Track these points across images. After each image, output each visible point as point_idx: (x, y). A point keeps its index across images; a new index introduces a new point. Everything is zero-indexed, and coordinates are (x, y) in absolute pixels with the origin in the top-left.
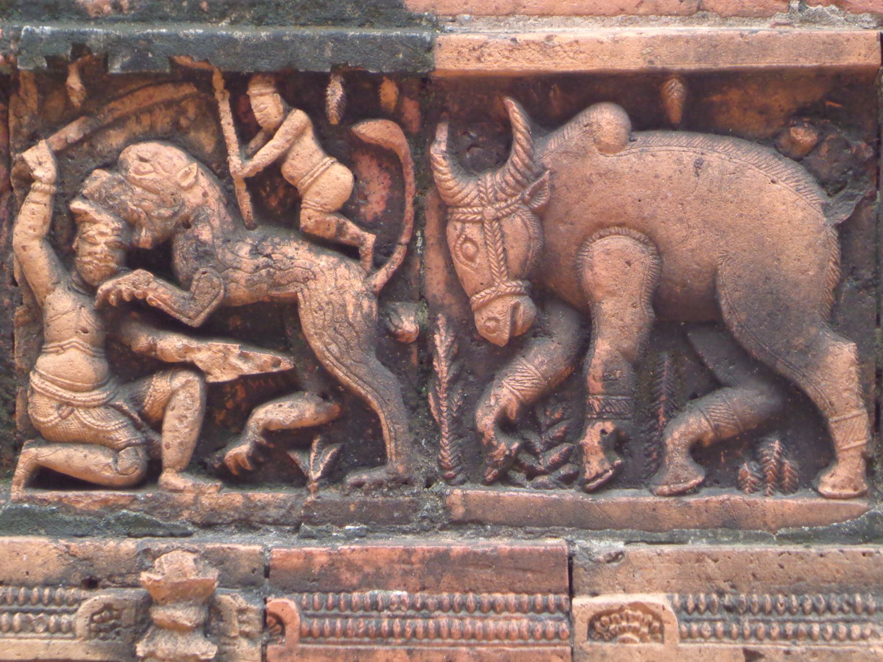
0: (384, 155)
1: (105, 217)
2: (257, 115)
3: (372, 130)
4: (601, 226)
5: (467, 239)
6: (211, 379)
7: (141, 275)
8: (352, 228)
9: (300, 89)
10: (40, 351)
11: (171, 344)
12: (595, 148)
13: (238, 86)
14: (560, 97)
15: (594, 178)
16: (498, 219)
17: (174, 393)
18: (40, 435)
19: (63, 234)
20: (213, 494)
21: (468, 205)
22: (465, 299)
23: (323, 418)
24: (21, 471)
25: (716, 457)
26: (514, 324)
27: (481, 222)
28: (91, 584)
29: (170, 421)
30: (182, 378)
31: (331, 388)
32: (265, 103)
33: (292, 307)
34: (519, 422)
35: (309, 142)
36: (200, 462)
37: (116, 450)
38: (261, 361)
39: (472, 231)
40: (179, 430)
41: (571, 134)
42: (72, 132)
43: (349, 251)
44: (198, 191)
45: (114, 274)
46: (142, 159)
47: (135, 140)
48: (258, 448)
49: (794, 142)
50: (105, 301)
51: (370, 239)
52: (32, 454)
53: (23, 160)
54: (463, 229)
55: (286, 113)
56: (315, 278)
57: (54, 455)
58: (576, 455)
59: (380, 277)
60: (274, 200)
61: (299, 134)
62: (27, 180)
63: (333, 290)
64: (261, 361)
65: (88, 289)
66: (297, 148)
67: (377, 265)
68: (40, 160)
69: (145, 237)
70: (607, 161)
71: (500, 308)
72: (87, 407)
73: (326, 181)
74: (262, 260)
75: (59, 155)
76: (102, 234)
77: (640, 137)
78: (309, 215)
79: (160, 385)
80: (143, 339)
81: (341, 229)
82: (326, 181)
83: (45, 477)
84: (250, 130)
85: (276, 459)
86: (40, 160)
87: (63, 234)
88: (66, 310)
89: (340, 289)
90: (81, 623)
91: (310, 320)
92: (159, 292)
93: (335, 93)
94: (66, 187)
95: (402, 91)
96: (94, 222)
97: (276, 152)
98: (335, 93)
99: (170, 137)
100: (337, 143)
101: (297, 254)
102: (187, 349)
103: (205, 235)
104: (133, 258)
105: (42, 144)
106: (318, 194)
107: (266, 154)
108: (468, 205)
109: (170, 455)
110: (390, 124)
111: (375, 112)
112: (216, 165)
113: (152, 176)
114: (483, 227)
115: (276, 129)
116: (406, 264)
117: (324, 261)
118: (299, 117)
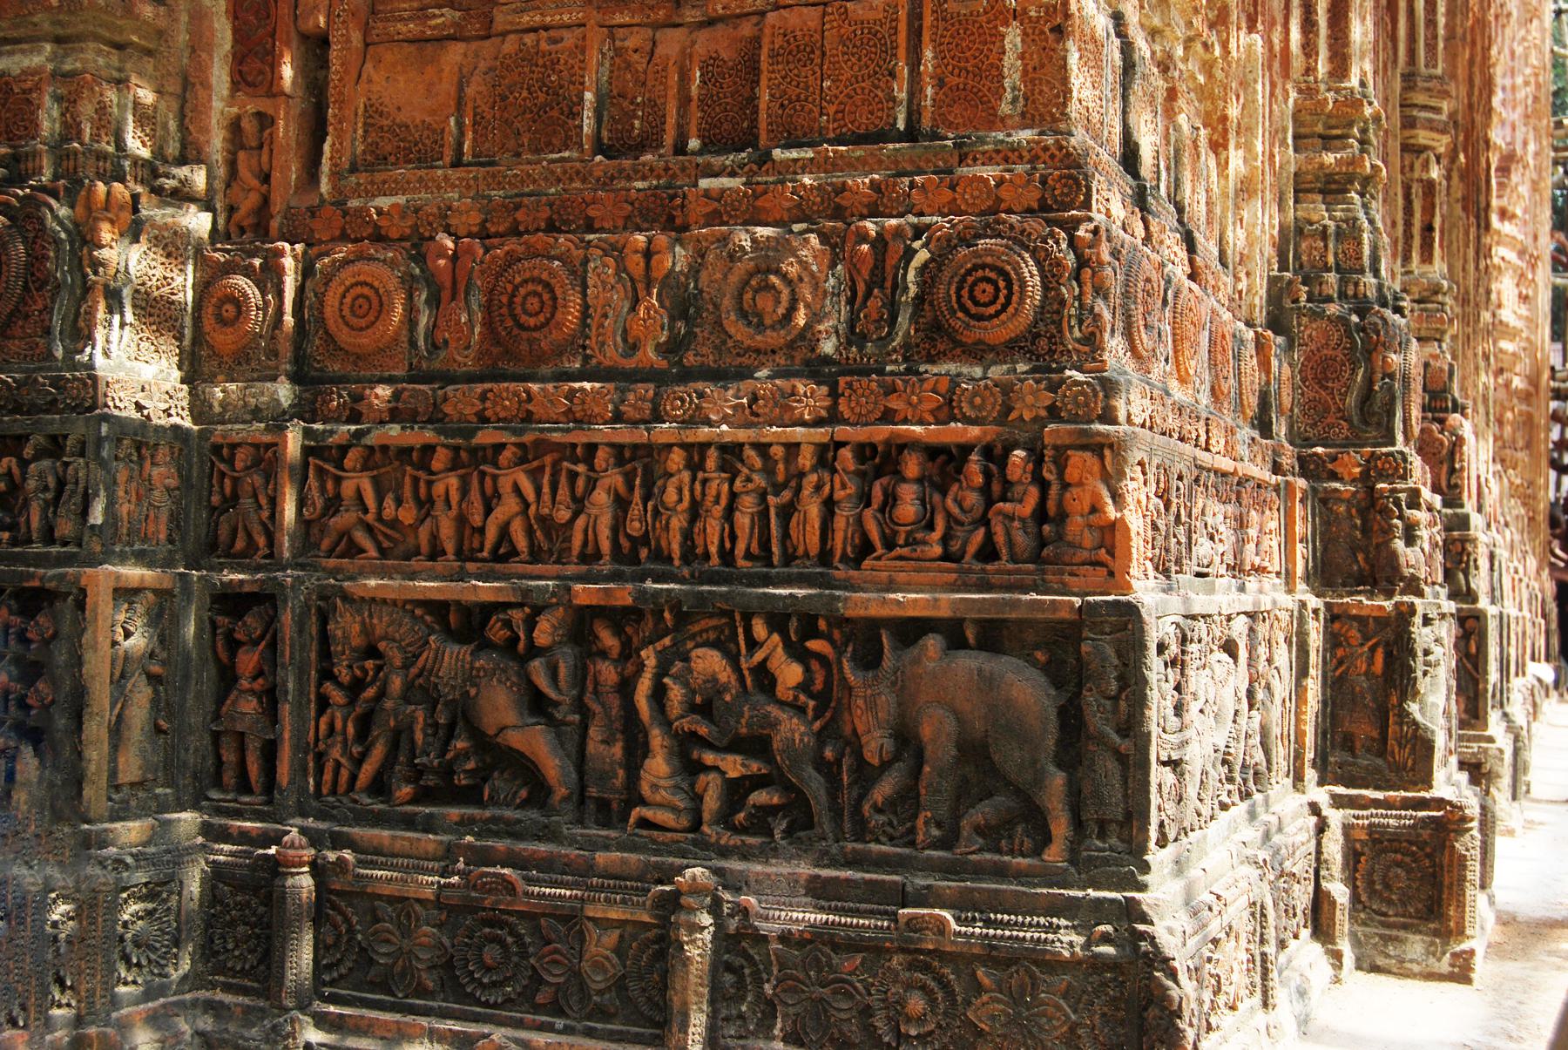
0: (821, 658)
3: (814, 645)
8: (802, 697)
9: (777, 622)
11: (709, 758)
13: (747, 618)
14: (911, 630)
18: (643, 802)
19: (659, 694)
20: (729, 839)
24: (632, 820)
25: (992, 835)
29: (707, 798)
30: (712, 776)
31: (788, 787)
32: (759, 629)
35: (780, 649)
36: (725, 818)
38: (755, 766)
40: (711, 802)
42: (667, 641)
43: (801, 710)
45: (682, 717)
47: (697, 646)
52: (637, 812)
55: (770, 633)
58: (912, 831)
59: (817, 725)
60: (765, 678)
63: (792, 730)
64: (755, 766)
67: (816, 718)
71: (876, 744)
72: (665, 788)
73: (790, 674)
75: (659, 653)
77: (952, 652)
78: (780, 691)
79: (703, 779)
81: (796, 698)
82: (790, 674)
83: (644, 823)
86: (649, 657)
87: (659, 694)
89: (793, 731)
90: (648, 903)
92: (703, 730)
93: (793, 624)
94: (662, 670)
95: (829, 625)
98: (793, 624)
99: (715, 645)
100: (798, 652)
101: (774, 711)
103: (728, 698)
104: (692, 708)
107: (759, 656)
109: (706, 816)
111: (816, 635)
112: (733, 660)
116: (832, 718)
118: (776, 637)
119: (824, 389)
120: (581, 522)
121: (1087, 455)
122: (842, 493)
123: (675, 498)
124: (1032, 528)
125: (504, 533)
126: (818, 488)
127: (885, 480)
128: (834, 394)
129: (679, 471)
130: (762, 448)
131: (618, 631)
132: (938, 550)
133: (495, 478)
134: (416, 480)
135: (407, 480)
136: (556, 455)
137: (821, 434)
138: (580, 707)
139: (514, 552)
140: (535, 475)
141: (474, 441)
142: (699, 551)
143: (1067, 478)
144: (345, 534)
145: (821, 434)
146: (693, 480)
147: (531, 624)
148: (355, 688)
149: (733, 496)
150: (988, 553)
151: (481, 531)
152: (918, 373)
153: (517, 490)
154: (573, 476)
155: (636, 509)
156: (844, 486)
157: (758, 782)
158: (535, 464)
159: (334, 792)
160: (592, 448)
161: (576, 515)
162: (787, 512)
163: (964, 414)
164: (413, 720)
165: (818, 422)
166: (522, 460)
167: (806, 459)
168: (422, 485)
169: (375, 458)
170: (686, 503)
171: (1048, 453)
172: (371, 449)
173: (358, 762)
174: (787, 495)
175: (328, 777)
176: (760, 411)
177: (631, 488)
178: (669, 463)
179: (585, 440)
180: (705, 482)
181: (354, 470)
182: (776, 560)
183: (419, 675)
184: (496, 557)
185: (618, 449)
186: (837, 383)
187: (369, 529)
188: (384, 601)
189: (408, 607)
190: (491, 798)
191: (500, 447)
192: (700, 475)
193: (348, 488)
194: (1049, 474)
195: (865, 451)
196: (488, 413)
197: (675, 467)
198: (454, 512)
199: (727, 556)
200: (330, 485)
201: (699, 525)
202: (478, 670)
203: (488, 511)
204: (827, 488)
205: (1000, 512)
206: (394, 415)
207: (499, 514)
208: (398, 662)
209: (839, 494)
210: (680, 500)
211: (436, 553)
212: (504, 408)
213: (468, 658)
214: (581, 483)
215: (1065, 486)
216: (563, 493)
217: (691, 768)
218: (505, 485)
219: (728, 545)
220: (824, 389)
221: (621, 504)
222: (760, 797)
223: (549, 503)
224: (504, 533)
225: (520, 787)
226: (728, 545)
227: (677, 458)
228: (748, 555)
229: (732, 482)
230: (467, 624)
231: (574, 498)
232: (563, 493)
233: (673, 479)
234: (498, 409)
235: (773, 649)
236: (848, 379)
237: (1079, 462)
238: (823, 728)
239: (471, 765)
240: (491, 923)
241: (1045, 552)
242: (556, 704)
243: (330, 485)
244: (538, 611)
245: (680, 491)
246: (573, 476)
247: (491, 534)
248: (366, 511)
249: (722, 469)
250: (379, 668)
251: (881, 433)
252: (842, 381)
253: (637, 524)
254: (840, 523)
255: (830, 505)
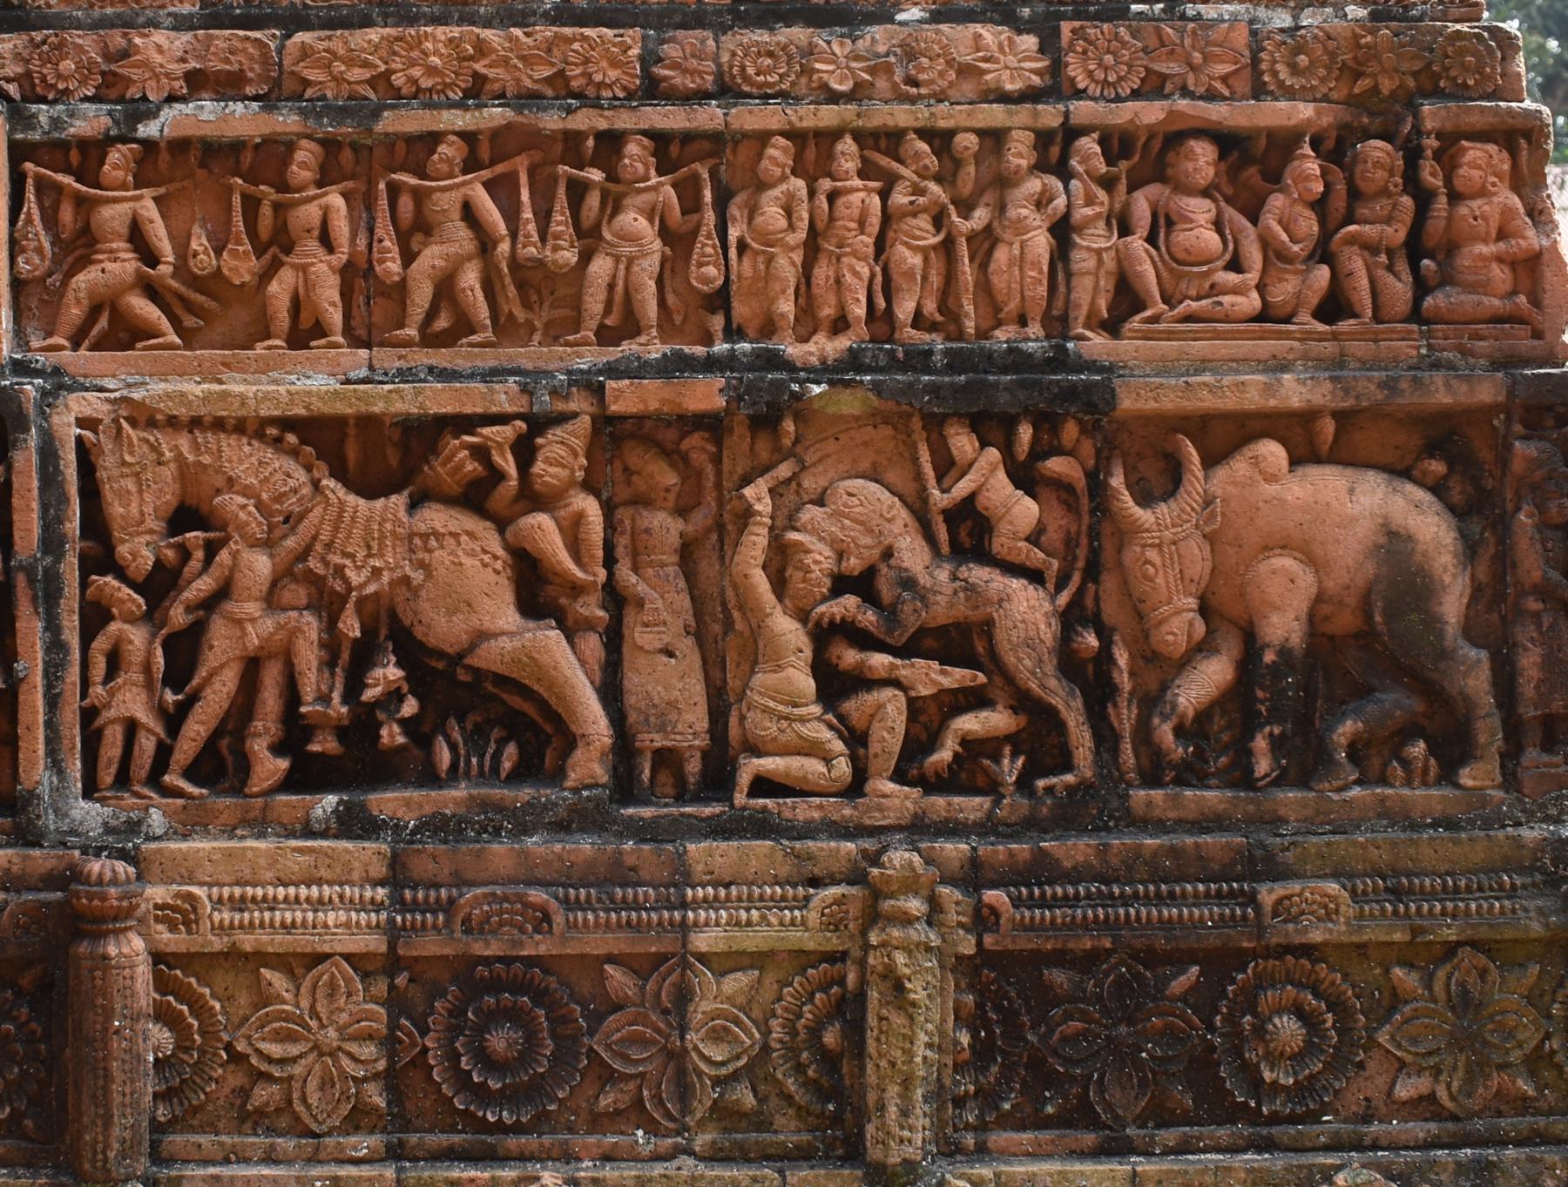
1: (821, 546)
2: (955, 452)
3: (1056, 465)
4: (1266, 548)
5: (1147, 562)
6: (913, 694)
7: (850, 601)
10: (753, 672)
12: (1259, 478)
14: (1224, 436)
15: (1261, 504)
16: (1174, 543)
17: (881, 706)
21: (1147, 530)
22: (1141, 617)
23: (1013, 729)
26: (1190, 636)
27: (1159, 546)
28: (815, 882)
30: (889, 692)
31: (1023, 702)
32: (962, 442)
33: (987, 627)
34: (1194, 730)
37: (827, 760)
38: (957, 677)
39: (1152, 554)
41: (1240, 466)
42: (784, 470)
43: (1035, 576)
44: (900, 523)
45: (825, 599)
46: (851, 495)
48: (956, 755)
49: (1425, 473)
50: (818, 624)
51: (1055, 564)
52: (750, 767)
53: (742, 497)
54: (1143, 553)
56: (1009, 600)
57: (770, 764)
58: (1244, 757)
59: (1063, 599)
61: (993, 470)
62: (746, 515)
63: (1026, 612)
65: (802, 616)
66: (992, 481)
67: (1059, 587)
68: (758, 494)
69: (854, 564)
70: (1271, 489)
74: (958, 583)
76: (817, 562)
78: (1001, 544)
80: (850, 657)
83: (764, 786)
84: (947, 467)
85: (971, 770)
88: (786, 628)
91: (1005, 639)
92: (869, 618)
93: (1025, 433)
96: (808, 551)
97: (973, 486)
98: (1025, 433)
100: (1025, 478)
102: (893, 667)
104: (841, 584)
105: (760, 481)
106: (1011, 523)
107: (962, 488)
108: (1147, 530)
110: (1071, 459)
113: (857, 510)
114: (1161, 551)
115: (970, 465)
117: (1016, 584)
118: (993, 454)
119: (1029, 42)
120: (600, 267)
121: (1492, 148)
122: (1088, 211)
123: (783, 223)
124: (1402, 266)
125: (445, 288)
126: (1041, 202)
127: (1154, 189)
128: (1049, 44)
129: (783, 178)
130: (940, 139)
131: (675, 457)
132: (1253, 302)
133: (419, 196)
134: (251, 205)
135: (237, 200)
136: (537, 156)
137: (1050, 115)
138: (616, 598)
139: (464, 326)
140: (501, 189)
141: (379, 127)
142: (827, 311)
143: (1458, 184)
144: (104, 304)
145: (1050, 115)
146: (812, 193)
147: (525, 451)
148: (159, 585)
149: (887, 218)
150: (1333, 307)
151: (401, 290)
152: (1183, 17)
153: (469, 213)
154: (577, 190)
155: (706, 245)
156: (1090, 201)
157: (974, 699)
158: (500, 168)
159: (123, 780)
160: (612, 141)
161: (586, 257)
162: (984, 242)
163: (1281, 84)
164: (295, 632)
165: (1031, 96)
166: (471, 164)
167: (1020, 152)
168: (266, 211)
169: (156, 164)
170: (801, 235)
171: (1431, 143)
172: (149, 145)
173: (174, 720)
174: (981, 216)
175: (112, 748)
176: (923, 77)
177: (691, 205)
178: (765, 163)
179: (603, 125)
180: (832, 197)
181: (124, 186)
182: (970, 326)
183: (306, 552)
184: (430, 340)
185: (660, 140)
186: (1056, 32)
187: (152, 291)
188: (219, 425)
189: (272, 431)
190: (454, 766)
191: (433, 139)
192: (826, 184)
193: (113, 216)
194: (1430, 175)
195: (1117, 144)
196: (398, 80)
197: (778, 171)
198: (341, 258)
199: (881, 320)
200: (67, 214)
201: (822, 272)
202: (425, 537)
203: (408, 258)
204: (1061, 201)
205: (1352, 240)
206: (197, 83)
207: (432, 257)
208: (258, 529)
209: (1082, 212)
210: (791, 227)
211: (304, 332)
212: (432, 71)
213: (402, 514)
214: (593, 200)
215: (1455, 197)
216: (560, 220)
217: (835, 685)
218: (447, 202)
219: (881, 303)
220: (1029, 42)
221: (678, 242)
222: (969, 723)
223: (536, 238)
224: (445, 288)
225: (501, 744)
226: (881, 303)
227: (778, 152)
228: (918, 320)
229: (884, 195)
230: (382, 456)
231: (580, 233)
232: (560, 220)
233: (776, 192)
234: (416, 72)
235: (985, 475)
236: (1077, 24)
237: (1479, 160)
238: (1071, 605)
239: (410, 707)
240: (495, 986)
241: (1429, 302)
242: (577, 589)
243: (67, 214)
244: (538, 424)
245: (789, 212)
246: (577, 190)
247: (422, 295)
248: (150, 257)
249: (862, 174)
250: (211, 549)
251: (1151, 113)
252: (1066, 27)
253: (711, 271)
254: (1082, 260)
255: (1063, 231)
